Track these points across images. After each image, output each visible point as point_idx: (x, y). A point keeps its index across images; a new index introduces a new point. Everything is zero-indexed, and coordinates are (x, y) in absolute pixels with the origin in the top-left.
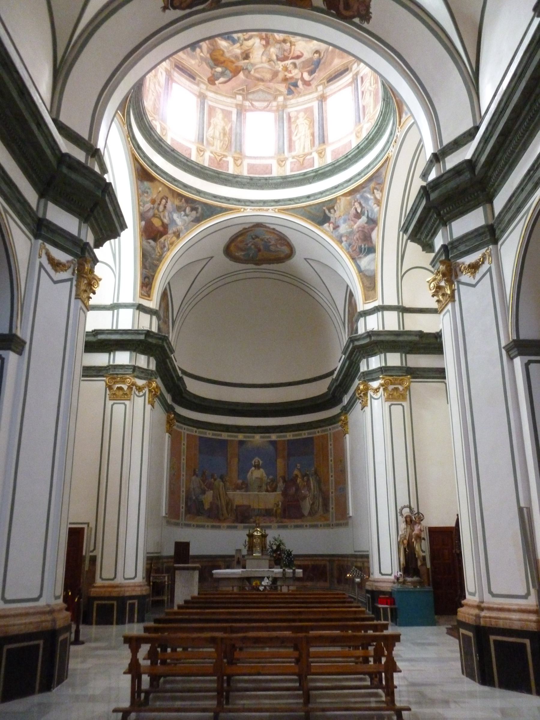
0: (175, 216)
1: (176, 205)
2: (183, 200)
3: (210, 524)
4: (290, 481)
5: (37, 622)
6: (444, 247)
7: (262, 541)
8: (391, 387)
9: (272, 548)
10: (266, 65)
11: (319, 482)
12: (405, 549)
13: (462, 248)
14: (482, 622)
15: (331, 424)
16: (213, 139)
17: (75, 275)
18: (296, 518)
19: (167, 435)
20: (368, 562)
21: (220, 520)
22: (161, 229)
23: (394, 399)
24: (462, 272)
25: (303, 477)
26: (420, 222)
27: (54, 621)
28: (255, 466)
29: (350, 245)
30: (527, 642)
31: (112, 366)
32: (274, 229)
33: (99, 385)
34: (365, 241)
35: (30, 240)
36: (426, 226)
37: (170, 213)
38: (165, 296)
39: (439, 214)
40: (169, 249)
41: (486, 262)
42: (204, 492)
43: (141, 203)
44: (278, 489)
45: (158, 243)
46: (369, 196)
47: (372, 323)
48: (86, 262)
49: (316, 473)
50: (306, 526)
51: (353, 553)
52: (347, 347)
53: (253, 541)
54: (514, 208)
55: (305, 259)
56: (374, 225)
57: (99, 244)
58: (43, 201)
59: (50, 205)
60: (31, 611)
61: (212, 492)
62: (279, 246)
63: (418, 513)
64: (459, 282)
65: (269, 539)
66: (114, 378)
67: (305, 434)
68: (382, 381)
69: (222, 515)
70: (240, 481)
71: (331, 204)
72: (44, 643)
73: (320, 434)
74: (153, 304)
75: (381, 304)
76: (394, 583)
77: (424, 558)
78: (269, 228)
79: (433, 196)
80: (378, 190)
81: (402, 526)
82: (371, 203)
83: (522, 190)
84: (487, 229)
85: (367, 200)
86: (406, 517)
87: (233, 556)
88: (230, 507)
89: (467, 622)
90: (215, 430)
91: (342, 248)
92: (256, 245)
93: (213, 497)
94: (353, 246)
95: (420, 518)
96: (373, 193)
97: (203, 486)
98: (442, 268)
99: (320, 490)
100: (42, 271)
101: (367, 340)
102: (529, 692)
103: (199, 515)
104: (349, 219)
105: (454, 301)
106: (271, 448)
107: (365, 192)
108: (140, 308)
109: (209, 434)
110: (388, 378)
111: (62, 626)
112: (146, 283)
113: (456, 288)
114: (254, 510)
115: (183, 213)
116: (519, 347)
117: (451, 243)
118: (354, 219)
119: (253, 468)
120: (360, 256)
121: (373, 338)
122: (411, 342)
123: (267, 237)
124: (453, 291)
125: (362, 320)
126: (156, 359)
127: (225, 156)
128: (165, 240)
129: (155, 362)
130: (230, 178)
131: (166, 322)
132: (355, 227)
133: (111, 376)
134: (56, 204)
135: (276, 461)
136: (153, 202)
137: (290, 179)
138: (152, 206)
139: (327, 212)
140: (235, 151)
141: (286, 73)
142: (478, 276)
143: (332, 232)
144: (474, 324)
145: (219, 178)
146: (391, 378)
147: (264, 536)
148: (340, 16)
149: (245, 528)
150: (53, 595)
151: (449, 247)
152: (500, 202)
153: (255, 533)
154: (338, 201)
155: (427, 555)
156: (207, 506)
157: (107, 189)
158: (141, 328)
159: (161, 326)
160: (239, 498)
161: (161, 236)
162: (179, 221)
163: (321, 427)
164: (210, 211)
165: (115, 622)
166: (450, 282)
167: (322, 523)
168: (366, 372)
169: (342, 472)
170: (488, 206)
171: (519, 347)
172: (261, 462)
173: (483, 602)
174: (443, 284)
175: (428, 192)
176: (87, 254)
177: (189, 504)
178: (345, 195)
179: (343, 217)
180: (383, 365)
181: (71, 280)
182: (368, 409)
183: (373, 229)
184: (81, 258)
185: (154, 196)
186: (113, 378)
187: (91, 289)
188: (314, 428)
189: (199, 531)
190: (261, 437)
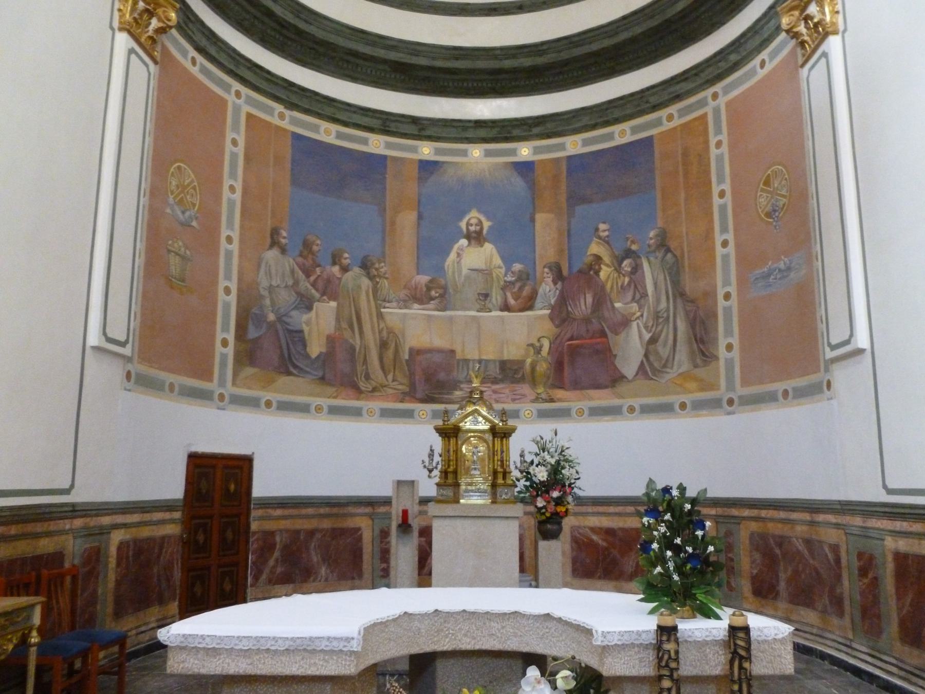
3: (325, 402)
4: (576, 278)
7: (492, 453)
9: (528, 476)
11: (675, 273)
15: (720, 77)
18: (598, 387)
19: (123, 41)
21: (358, 392)
28: (468, 237)
42: (306, 304)
44: (539, 302)
49: (663, 244)
53: (457, 451)
61: (333, 304)
65: (522, 443)
67: (622, 134)
69: (367, 377)
70: (423, 279)
87: (387, 502)
88: (390, 353)
90: (345, 124)
93: (338, 320)
97: (305, 285)
99: (679, 293)
103: (289, 373)
106: (518, 183)
109: (328, 133)
114: (466, 361)
119: (464, 242)
135: (533, 220)
147: (500, 434)
153: (468, 425)
156: (316, 348)
160: (419, 327)
163: (678, 98)
167: (687, 398)
172: (486, 224)
177: (252, 333)
189: (292, 423)
190: (488, 153)
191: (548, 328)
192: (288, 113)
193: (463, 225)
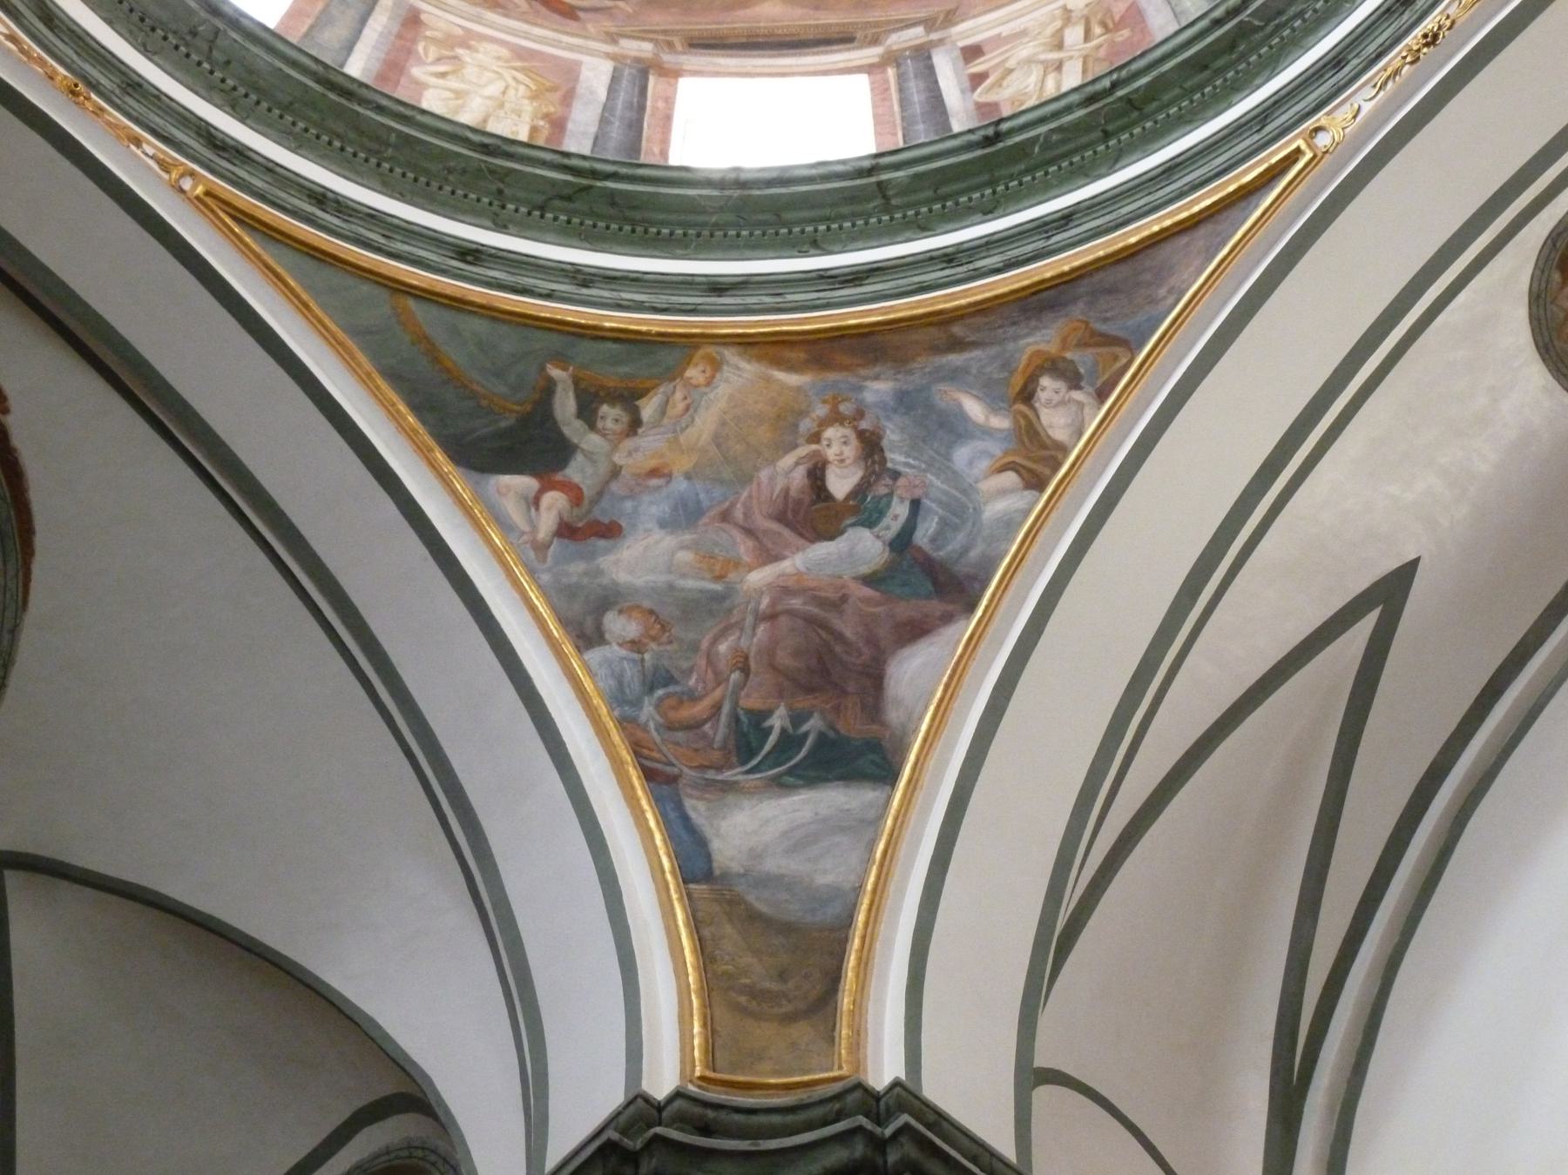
29: (657, 679)
34: (810, 690)
56: (936, 607)
71: (630, 370)
94: (693, 698)
96: (1027, 395)
104: (725, 516)
107: (955, 376)
132: (759, 577)
139: (565, 405)
143: (541, 548)
154: (694, 373)
179: (680, 485)
183: (915, 631)
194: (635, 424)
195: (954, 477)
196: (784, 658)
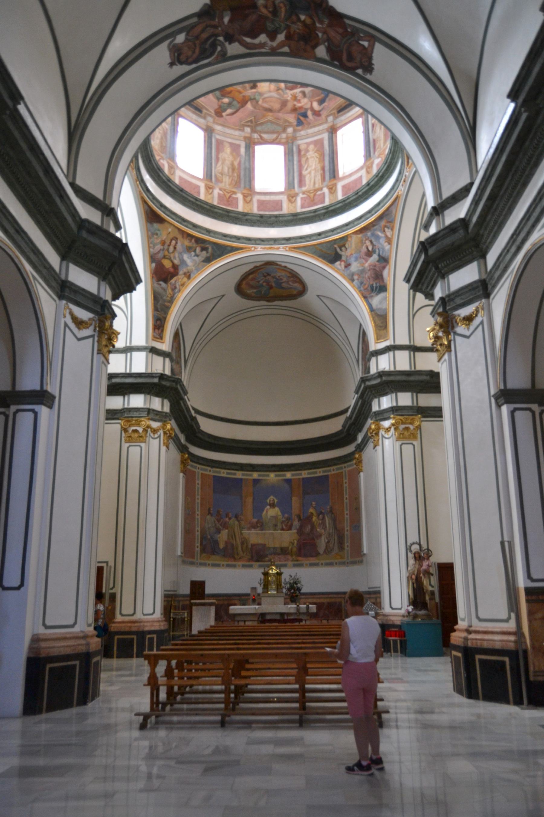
0: (186, 257)
1: (187, 246)
2: (193, 241)
3: (225, 563)
5: (74, 645)
6: (442, 299)
7: (277, 579)
8: (402, 427)
10: (274, 94)
11: (334, 520)
12: (413, 584)
13: (458, 301)
14: (470, 644)
15: (346, 462)
16: (222, 174)
17: (97, 331)
18: (312, 556)
19: (181, 475)
20: (380, 598)
21: (235, 559)
22: (172, 270)
23: (404, 438)
24: (458, 324)
25: (318, 515)
26: (421, 274)
27: (88, 644)
29: (362, 283)
30: (507, 659)
31: (127, 409)
32: (285, 267)
33: (114, 428)
35: (55, 301)
36: (427, 277)
37: (180, 253)
38: (177, 336)
39: (437, 268)
40: (179, 291)
41: (479, 315)
42: (219, 531)
43: (151, 245)
44: (293, 528)
45: (169, 284)
46: (380, 234)
47: (384, 363)
48: (106, 318)
49: (331, 511)
50: (322, 564)
51: (367, 590)
52: (359, 387)
53: (268, 579)
54: (502, 267)
55: (318, 296)
56: (385, 264)
57: (116, 297)
58: (64, 263)
59: (72, 267)
60: (68, 636)
61: (227, 531)
62: (291, 283)
63: (428, 549)
64: (455, 333)
66: (129, 421)
67: (319, 472)
68: (393, 421)
69: (238, 554)
70: (255, 520)
72: (80, 664)
73: (335, 472)
74: (165, 346)
75: (392, 343)
76: (403, 616)
77: (432, 593)
78: (280, 265)
79: (431, 251)
80: (388, 228)
81: (412, 561)
82: (382, 241)
83: (508, 251)
84: (480, 284)
85: (378, 238)
86: (415, 554)
87: (248, 595)
88: (245, 546)
89: (458, 644)
90: (228, 469)
91: (353, 287)
92: (268, 283)
94: (365, 284)
95: (429, 554)
96: (384, 231)
97: (218, 525)
98: (439, 319)
99: (335, 528)
100: (67, 330)
101: (378, 381)
102: (507, 702)
103: (214, 554)
104: (360, 258)
105: (451, 351)
107: (376, 230)
108: (153, 351)
109: (223, 473)
110: (398, 417)
111: (94, 650)
112: (158, 325)
113: (452, 338)
114: (270, 548)
115: (193, 253)
116: (505, 396)
117: (449, 296)
118: (365, 257)
119: (268, 507)
120: (372, 294)
121: (384, 378)
122: (422, 381)
123: (279, 274)
124: (449, 342)
125: (373, 360)
126: (170, 401)
127: (235, 193)
128: (175, 282)
129: (169, 404)
130: (240, 216)
131: (178, 363)
133: (127, 419)
134: (77, 265)
135: (291, 499)
136: (163, 243)
137: (301, 217)
138: (162, 247)
139: (338, 250)
140: (245, 188)
141: (295, 103)
142: (472, 328)
143: (344, 270)
144: (470, 372)
145: (228, 216)
146: (402, 418)
147: (279, 574)
148: (343, 67)
149: (260, 566)
150: (85, 625)
151: (447, 299)
152: (491, 258)
153: (270, 572)
154: (349, 239)
155: (436, 590)
156: (222, 546)
157: (124, 248)
158: (155, 371)
159: (174, 367)
160: (254, 537)
161: (172, 278)
162: (189, 262)
164: (221, 251)
165: (135, 655)
166: (447, 333)
167: (336, 561)
168: (377, 411)
169: (356, 510)
170: (482, 261)
171: (505, 396)
172: (276, 501)
173: (471, 626)
174: (440, 334)
175: (426, 247)
176: (106, 311)
177: (204, 543)
178: (356, 233)
179: (354, 255)
180: (395, 404)
181: (93, 336)
182: (379, 448)
183: (384, 268)
184: (101, 315)
185: (164, 237)
186: (128, 420)
187: (111, 343)
188: (329, 466)
190: (276, 476)
191: (296, 536)
192: (212, 469)
193: (268, 501)
194: (346, 249)
195: (381, 244)
196: (373, 276)
